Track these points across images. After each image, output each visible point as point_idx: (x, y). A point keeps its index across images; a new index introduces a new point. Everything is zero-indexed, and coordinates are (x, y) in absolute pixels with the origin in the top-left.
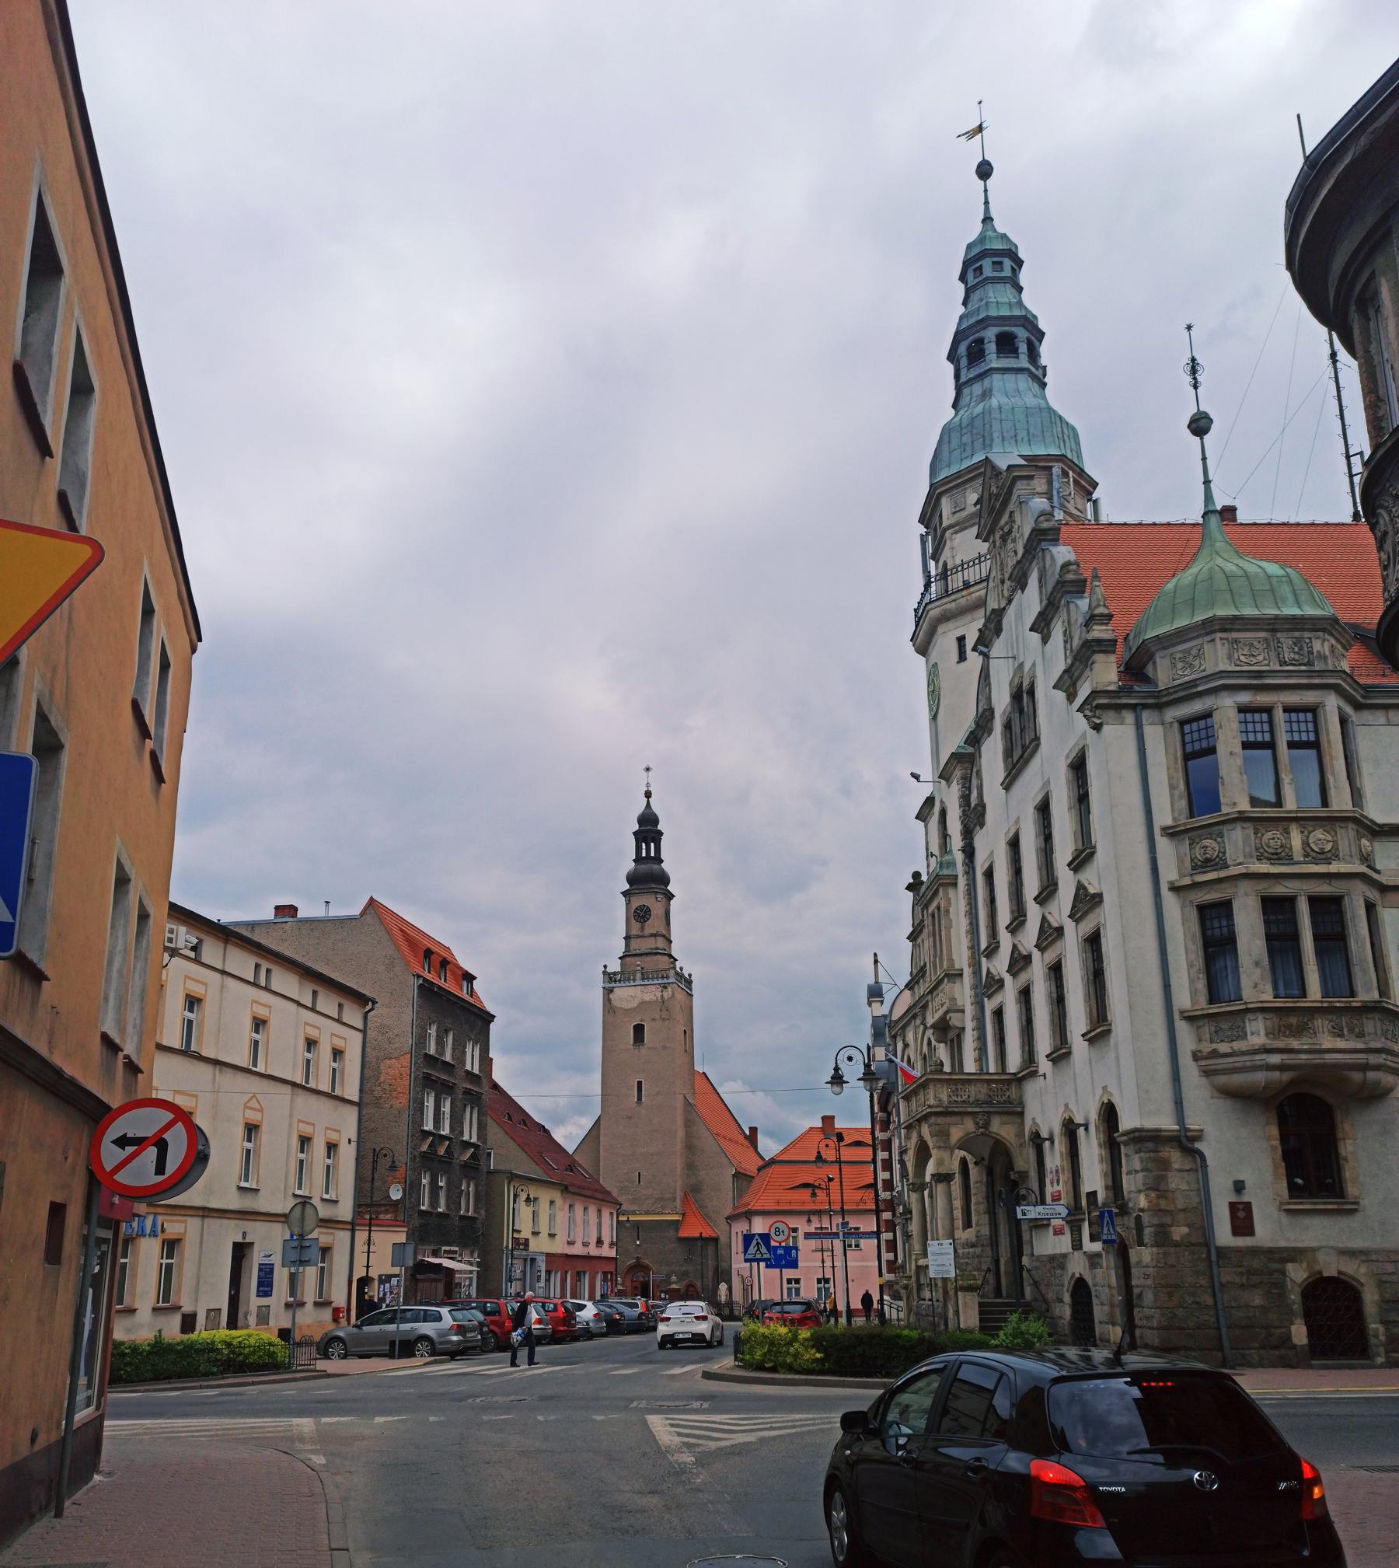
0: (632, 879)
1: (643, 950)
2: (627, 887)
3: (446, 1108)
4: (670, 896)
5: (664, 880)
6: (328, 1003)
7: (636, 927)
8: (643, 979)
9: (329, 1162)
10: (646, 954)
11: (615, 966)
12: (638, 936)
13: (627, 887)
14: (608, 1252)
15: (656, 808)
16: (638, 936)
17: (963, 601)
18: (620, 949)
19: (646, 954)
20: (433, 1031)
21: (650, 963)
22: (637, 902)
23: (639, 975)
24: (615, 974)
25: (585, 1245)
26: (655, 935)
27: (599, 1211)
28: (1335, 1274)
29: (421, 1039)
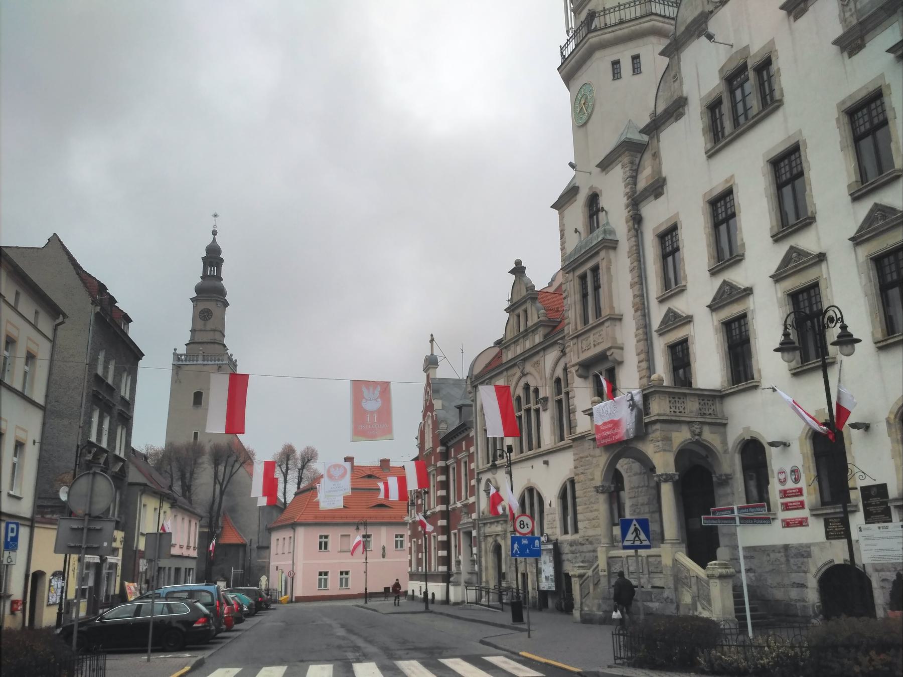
0: (198, 289)
1: (205, 340)
2: (195, 295)
3: (106, 426)
4: (226, 304)
5: (222, 292)
6: (27, 307)
7: (200, 324)
8: (204, 360)
9: (15, 459)
10: (208, 343)
11: (182, 350)
12: (201, 330)
13: (195, 295)
14: (194, 554)
15: (219, 242)
16: (201, 330)
17: (619, 33)
18: (187, 338)
19: (208, 343)
20: (101, 357)
21: (210, 349)
22: (203, 306)
23: (200, 357)
24: (181, 355)
25: (181, 547)
26: (214, 330)
27: (190, 521)
28: (842, 562)
29: (93, 364)
